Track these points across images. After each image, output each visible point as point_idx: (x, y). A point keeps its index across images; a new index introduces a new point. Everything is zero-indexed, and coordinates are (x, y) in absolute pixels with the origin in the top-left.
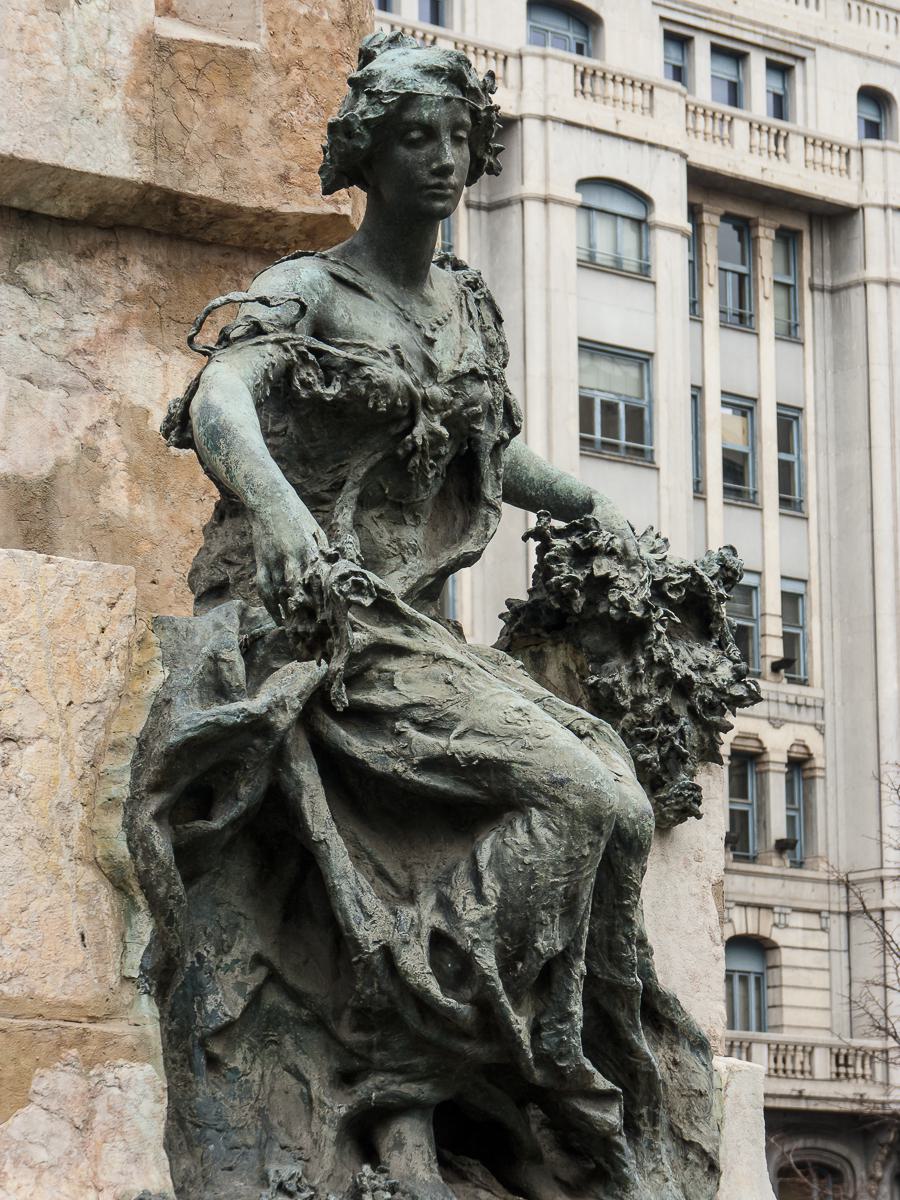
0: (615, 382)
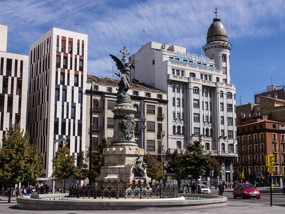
0: (197, 102)
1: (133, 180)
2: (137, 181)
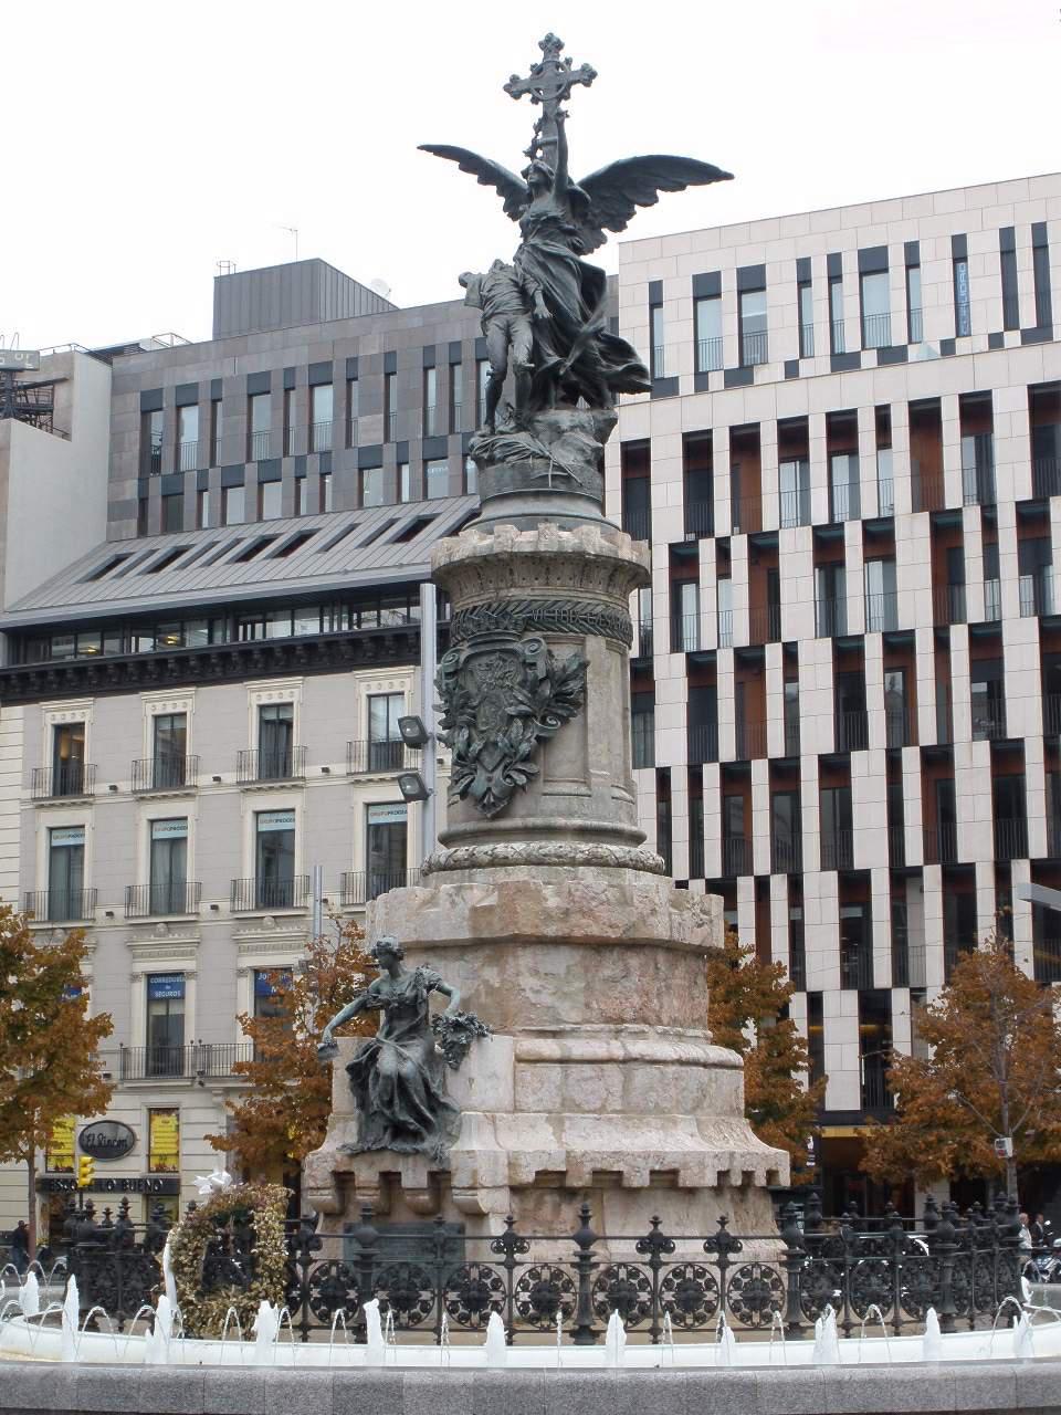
1: (330, 1166)
2: (366, 1174)
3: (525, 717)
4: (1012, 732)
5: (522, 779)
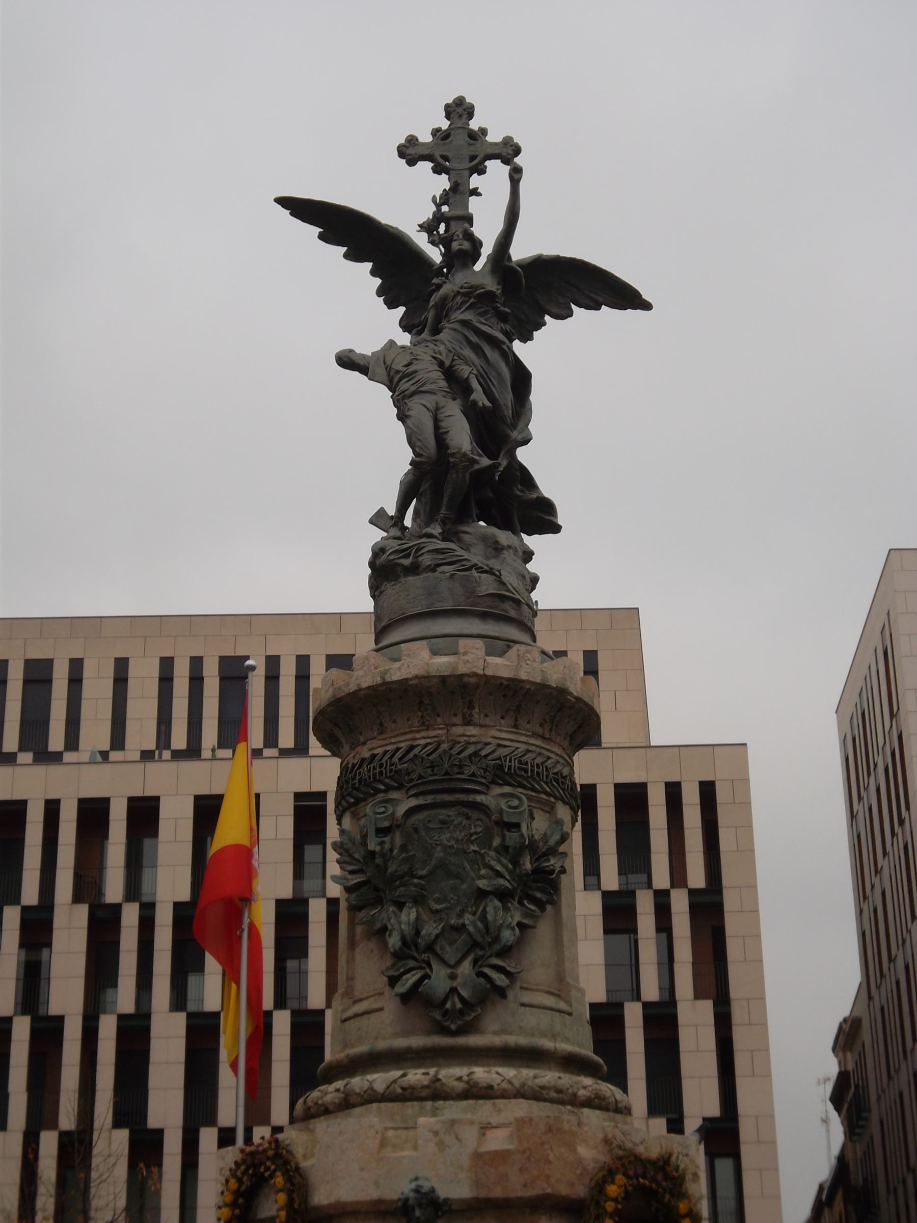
3: (503, 895)
4: (153, 1122)
5: (500, 979)
